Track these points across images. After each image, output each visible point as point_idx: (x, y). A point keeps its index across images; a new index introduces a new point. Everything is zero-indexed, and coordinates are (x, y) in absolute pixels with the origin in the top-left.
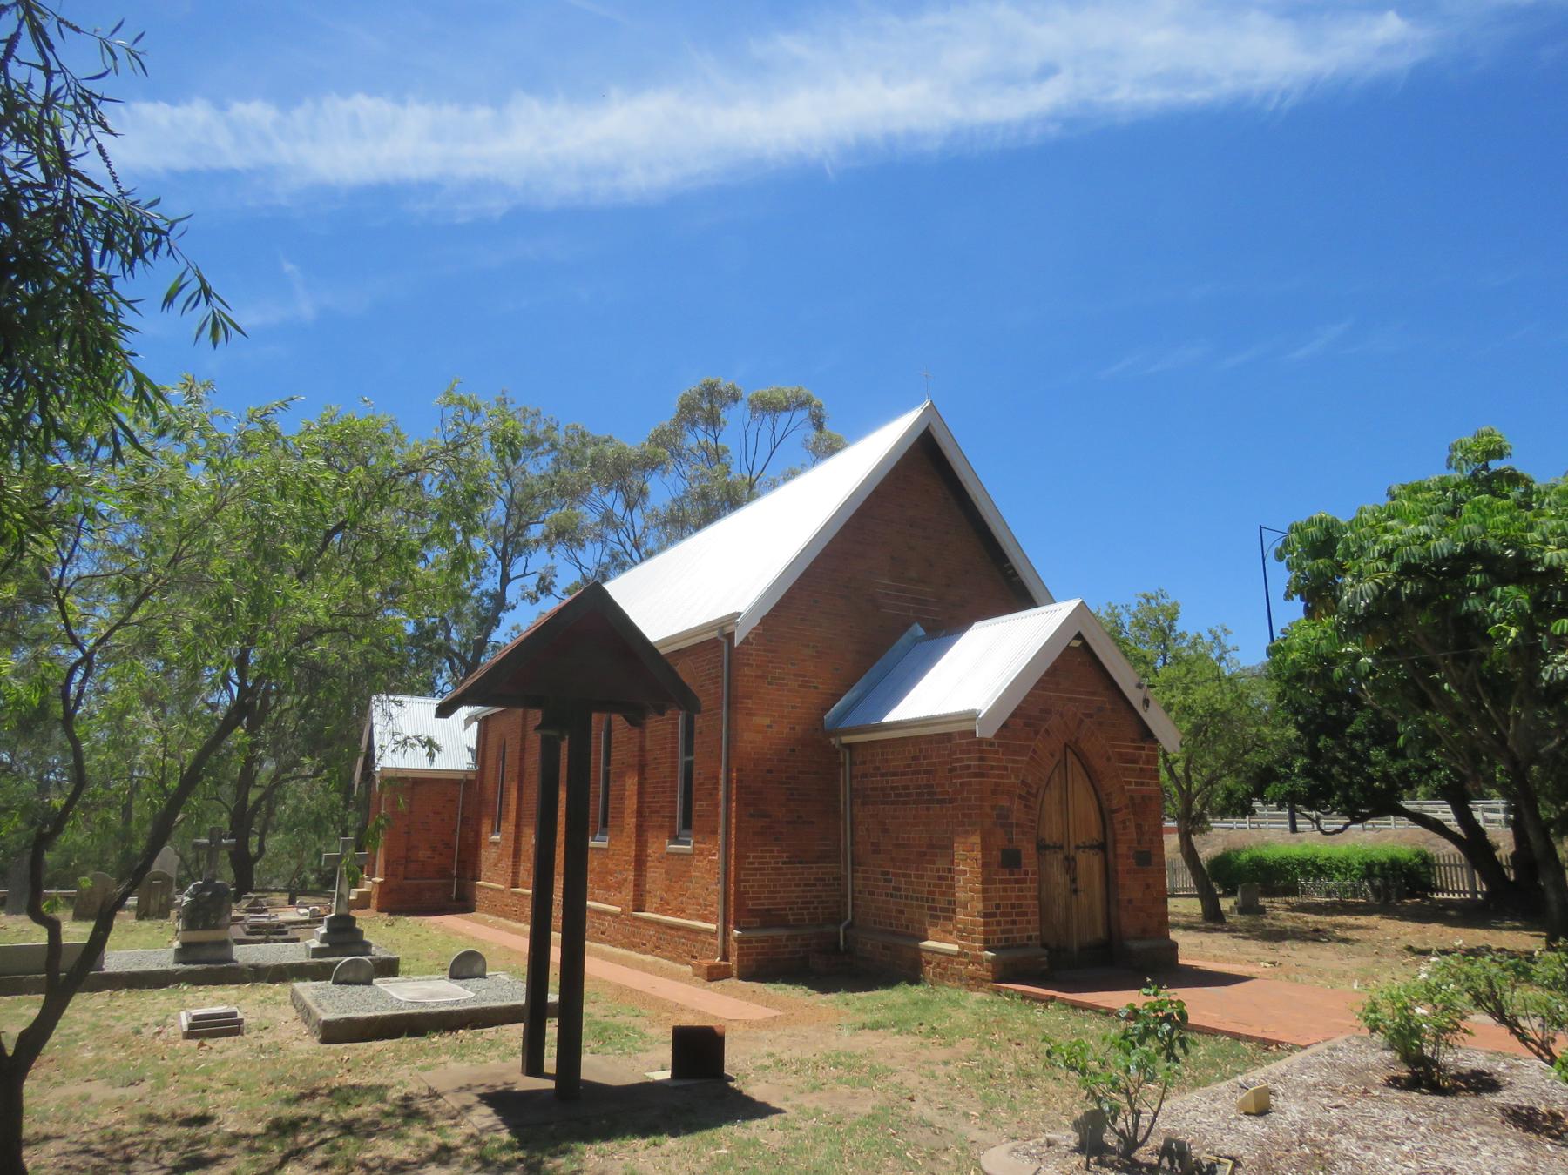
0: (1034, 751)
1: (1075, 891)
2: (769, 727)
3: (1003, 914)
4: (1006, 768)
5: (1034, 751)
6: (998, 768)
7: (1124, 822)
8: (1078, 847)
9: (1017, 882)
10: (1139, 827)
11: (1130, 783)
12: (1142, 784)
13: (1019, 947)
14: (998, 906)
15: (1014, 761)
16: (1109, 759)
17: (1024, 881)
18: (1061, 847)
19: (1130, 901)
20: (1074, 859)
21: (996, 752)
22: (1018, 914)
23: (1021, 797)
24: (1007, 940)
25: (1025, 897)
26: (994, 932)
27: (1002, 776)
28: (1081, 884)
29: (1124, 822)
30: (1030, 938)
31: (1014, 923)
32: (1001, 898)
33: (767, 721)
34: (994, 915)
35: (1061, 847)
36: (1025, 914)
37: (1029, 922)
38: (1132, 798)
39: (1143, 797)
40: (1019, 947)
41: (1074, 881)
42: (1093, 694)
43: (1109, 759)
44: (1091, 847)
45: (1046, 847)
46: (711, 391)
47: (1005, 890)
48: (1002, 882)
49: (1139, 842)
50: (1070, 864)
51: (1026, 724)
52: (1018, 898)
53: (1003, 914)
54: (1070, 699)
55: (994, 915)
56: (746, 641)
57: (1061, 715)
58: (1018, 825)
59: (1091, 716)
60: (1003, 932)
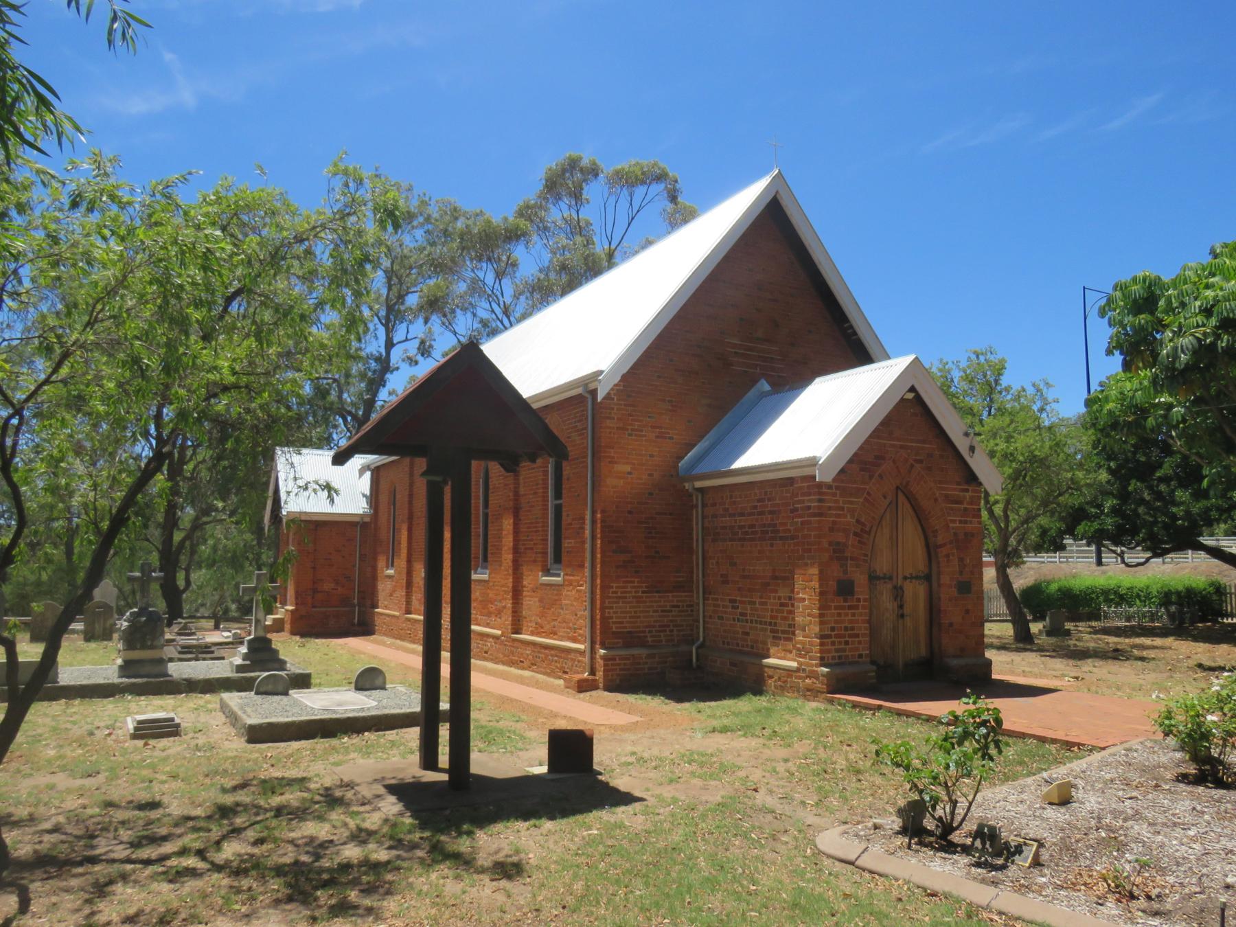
0: (869, 493)
2: (630, 473)
3: (837, 636)
4: (843, 509)
5: (869, 493)
7: (948, 556)
8: (905, 578)
9: (850, 608)
10: (961, 560)
11: (954, 521)
12: (966, 522)
13: (850, 663)
14: (833, 629)
15: (852, 503)
17: (856, 607)
18: (891, 578)
19: (951, 625)
20: (901, 588)
21: (834, 495)
22: (850, 636)
24: (840, 657)
26: (829, 651)
27: (838, 516)
28: (907, 610)
29: (948, 556)
30: (860, 656)
31: (847, 643)
33: (628, 468)
34: (829, 636)
35: (891, 578)
36: (857, 636)
37: (860, 642)
39: (966, 534)
40: (850, 663)
41: (901, 607)
43: (936, 500)
44: (917, 578)
45: (878, 578)
46: (573, 164)
47: (839, 615)
49: (961, 573)
50: (898, 593)
51: (862, 470)
52: (851, 621)
53: (837, 636)
54: (901, 447)
55: (829, 636)
56: (608, 397)
58: (852, 559)
59: (920, 462)
60: (837, 651)
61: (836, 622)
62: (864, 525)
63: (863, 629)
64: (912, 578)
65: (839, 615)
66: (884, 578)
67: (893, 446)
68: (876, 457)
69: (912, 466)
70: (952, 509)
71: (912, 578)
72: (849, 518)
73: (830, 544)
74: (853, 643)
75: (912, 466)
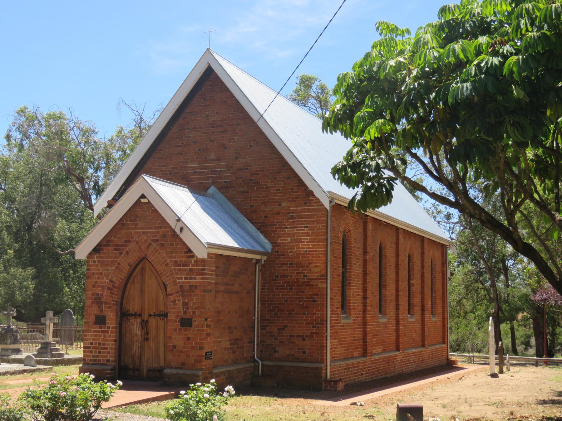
0: (119, 264)
1: (147, 339)
3: (94, 348)
4: (101, 274)
5: (119, 264)
6: (97, 274)
7: (175, 301)
9: (103, 332)
11: (181, 278)
12: (191, 278)
14: (91, 344)
15: (108, 270)
16: (167, 265)
17: (107, 332)
19: (175, 347)
20: (147, 321)
21: (97, 266)
22: (102, 348)
23: (109, 288)
24: (95, 360)
25: (107, 340)
26: (88, 356)
27: (99, 278)
28: (151, 335)
29: (175, 301)
30: (108, 361)
31: (100, 352)
32: (93, 340)
34: (89, 348)
35: (140, 315)
36: (107, 349)
38: (181, 287)
39: (191, 286)
40: (101, 364)
41: (147, 333)
42: (160, 228)
43: (167, 265)
44: (159, 315)
47: (96, 336)
48: (94, 331)
49: (185, 313)
51: (115, 250)
52: (103, 340)
53: (94, 348)
54: (143, 233)
55: (89, 348)
57: (137, 243)
58: (106, 303)
59: (156, 241)
60: (93, 356)
61: (94, 340)
62: (114, 282)
63: (111, 345)
64: (155, 315)
65: (96, 336)
66: (135, 315)
68: (126, 241)
69: (150, 244)
70: (179, 270)
71: (155, 315)
72: (105, 279)
73: (93, 294)
74: (104, 353)
75: (150, 244)
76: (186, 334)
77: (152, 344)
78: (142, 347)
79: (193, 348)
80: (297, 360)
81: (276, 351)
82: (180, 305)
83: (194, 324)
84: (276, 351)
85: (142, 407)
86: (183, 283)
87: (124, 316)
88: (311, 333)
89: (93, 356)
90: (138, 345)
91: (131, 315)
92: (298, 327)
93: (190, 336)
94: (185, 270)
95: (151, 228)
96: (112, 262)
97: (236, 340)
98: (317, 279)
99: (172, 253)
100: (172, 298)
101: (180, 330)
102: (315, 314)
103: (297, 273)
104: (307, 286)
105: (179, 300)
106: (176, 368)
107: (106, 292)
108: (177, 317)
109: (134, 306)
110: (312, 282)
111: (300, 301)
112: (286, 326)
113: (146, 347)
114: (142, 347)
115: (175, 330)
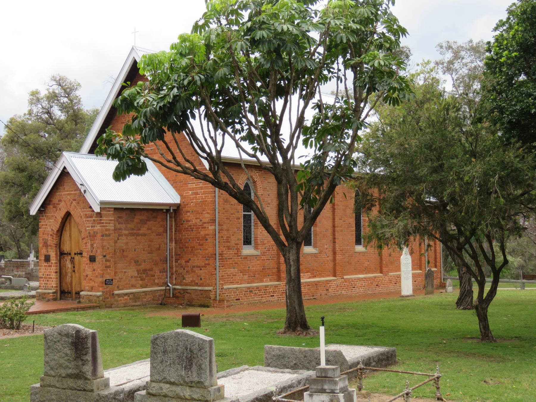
3: (45, 278)
5: (56, 217)
7: (86, 243)
8: (75, 254)
9: (49, 266)
10: (92, 245)
12: (94, 226)
18: (70, 254)
25: (51, 272)
27: (46, 228)
29: (86, 243)
35: (70, 254)
38: (89, 233)
41: (74, 267)
43: (81, 217)
47: (45, 269)
50: (72, 261)
53: (45, 278)
54: (68, 194)
57: (65, 202)
60: (45, 284)
61: (45, 272)
64: (78, 254)
67: (65, 195)
69: (72, 202)
70: (88, 221)
71: (78, 254)
76: (93, 267)
77: (77, 275)
78: (72, 277)
79: (97, 277)
80: (197, 285)
81: (184, 279)
82: (89, 246)
83: (96, 260)
84: (184, 279)
85: (50, 316)
86: (90, 230)
87: (62, 254)
88: (205, 264)
89: (45, 284)
90: (69, 275)
91: (65, 254)
92: (198, 260)
93: (95, 268)
94: (91, 221)
95: (72, 191)
96: (52, 216)
97: (145, 270)
98: (208, 223)
99: (84, 209)
100: (85, 241)
101: (90, 264)
102: (207, 249)
103: (196, 219)
104: (202, 228)
105: (88, 243)
106: (88, 291)
107: (50, 238)
108: (87, 255)
109: (66, 248)
110: (205, 225)
111: (198, 240)
112: (190, 259)
113: (74, 276)
114: (72, 277)
115: (87, 264)
